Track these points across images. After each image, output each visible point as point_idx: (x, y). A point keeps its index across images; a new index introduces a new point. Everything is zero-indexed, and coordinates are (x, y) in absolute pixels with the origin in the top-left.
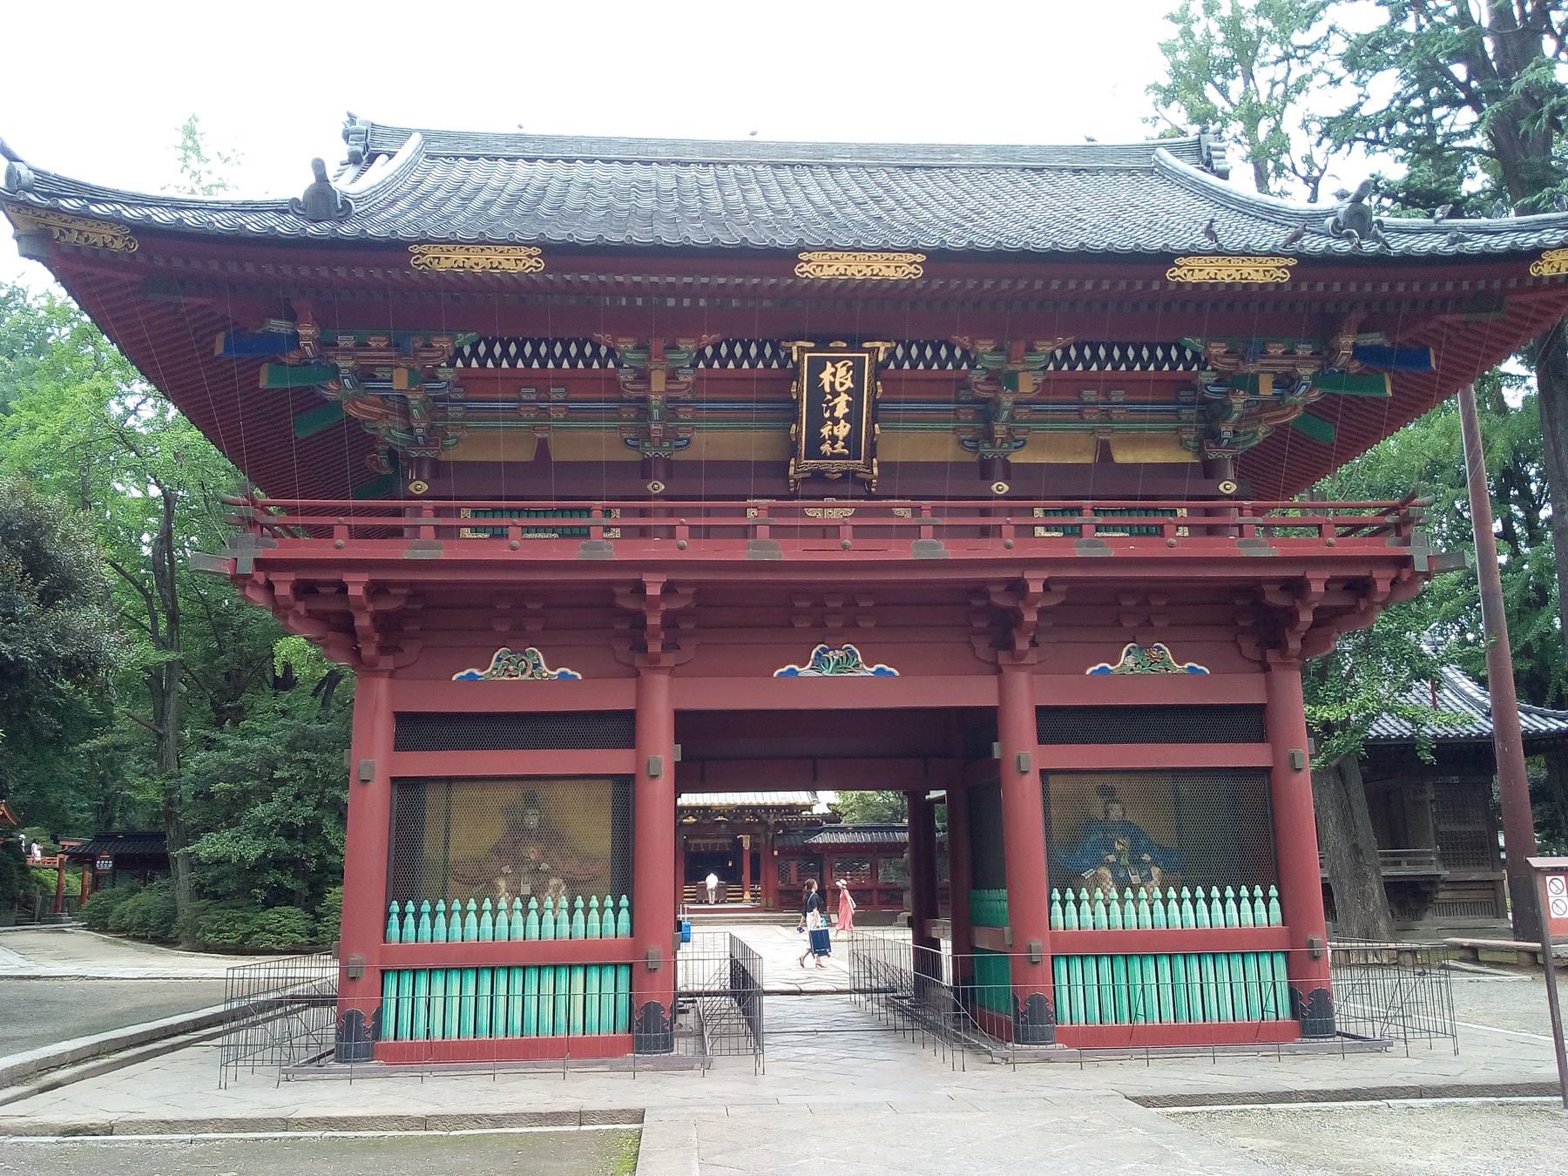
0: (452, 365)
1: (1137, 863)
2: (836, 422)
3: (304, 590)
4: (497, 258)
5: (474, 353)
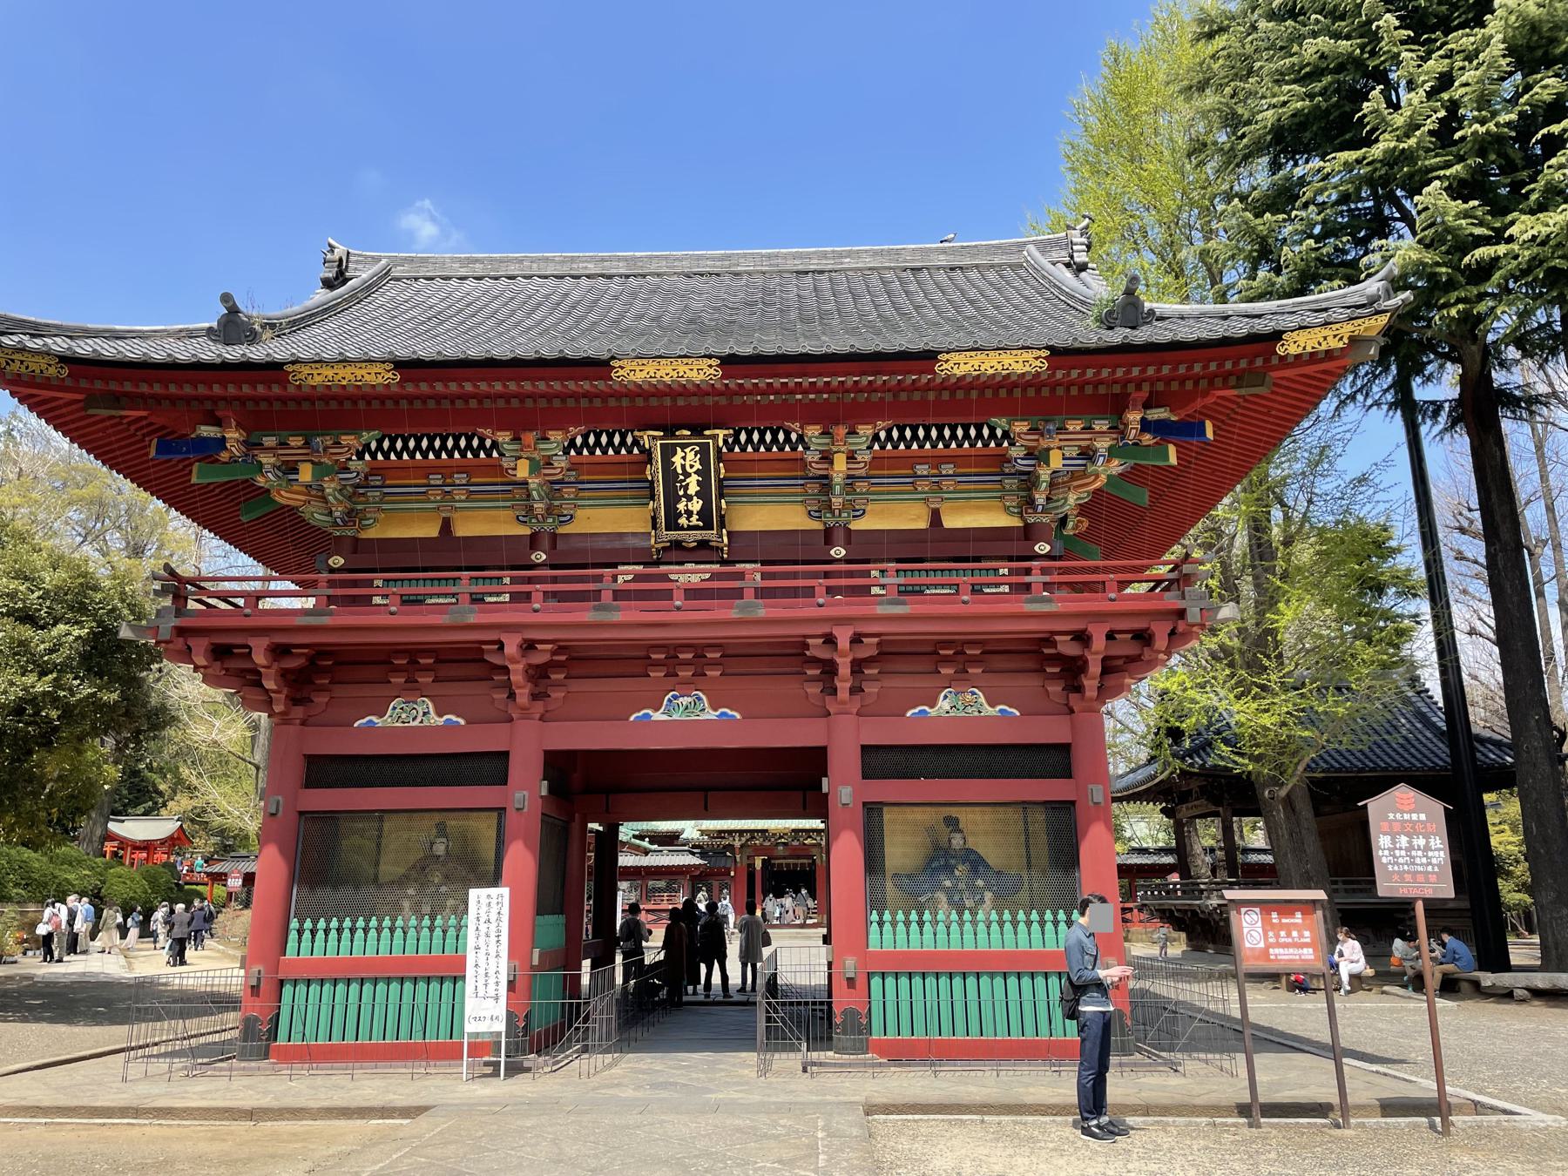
1: (973, 889)
2: (690, 498)
4: (359, 373)
5: (380, 447)
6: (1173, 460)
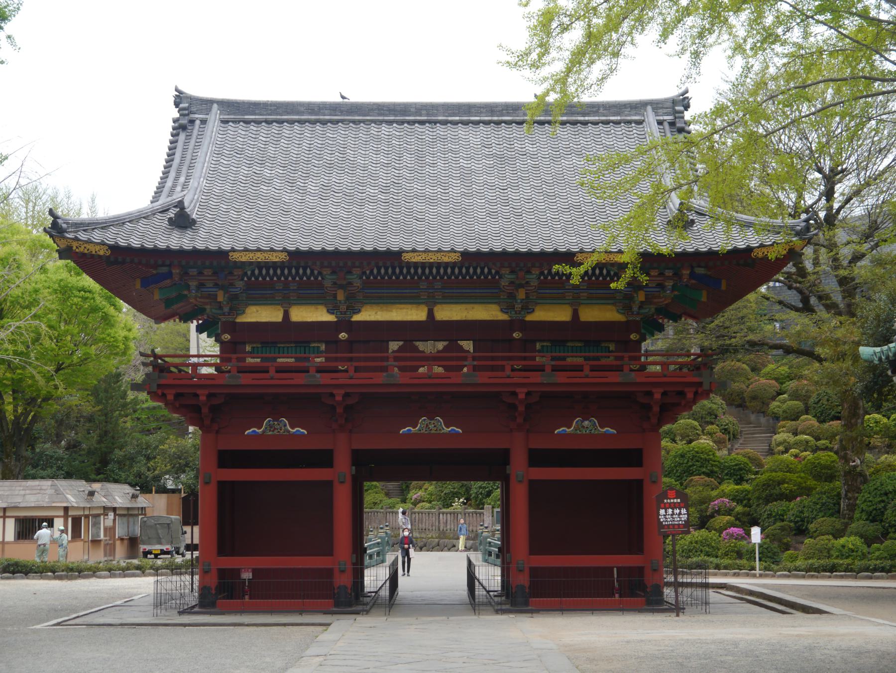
0: (242, 279)
3: (178, 396)
6: (704, 299)
